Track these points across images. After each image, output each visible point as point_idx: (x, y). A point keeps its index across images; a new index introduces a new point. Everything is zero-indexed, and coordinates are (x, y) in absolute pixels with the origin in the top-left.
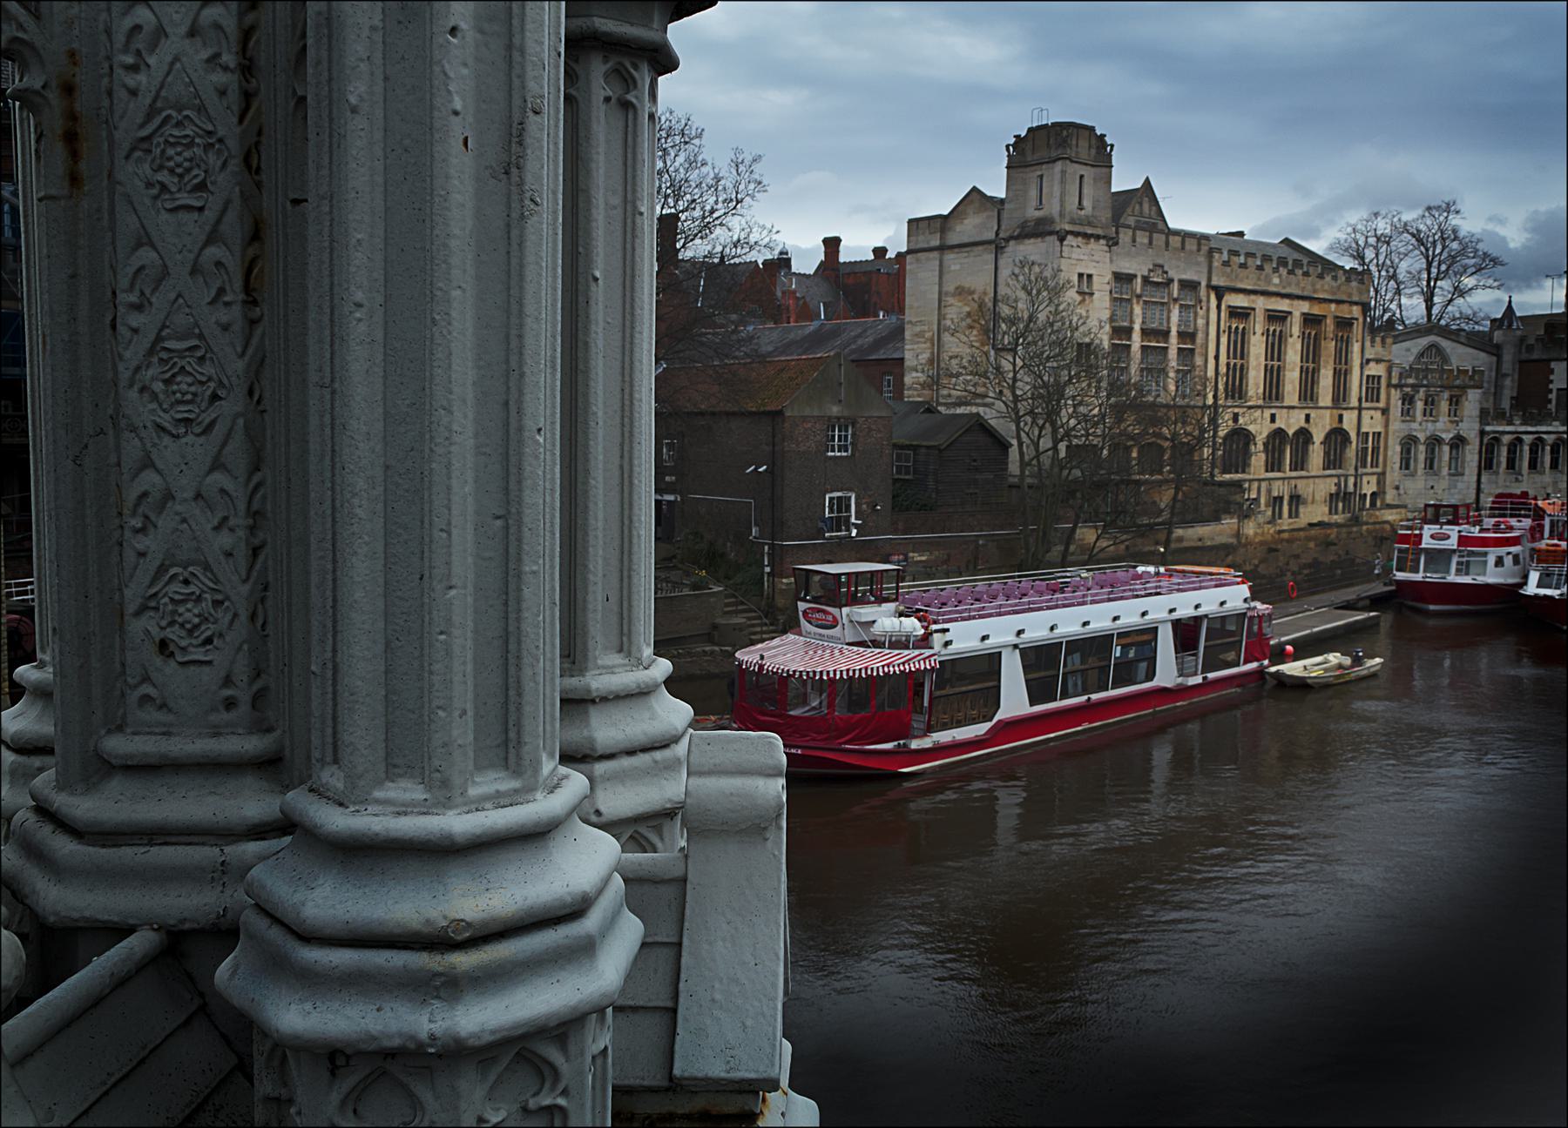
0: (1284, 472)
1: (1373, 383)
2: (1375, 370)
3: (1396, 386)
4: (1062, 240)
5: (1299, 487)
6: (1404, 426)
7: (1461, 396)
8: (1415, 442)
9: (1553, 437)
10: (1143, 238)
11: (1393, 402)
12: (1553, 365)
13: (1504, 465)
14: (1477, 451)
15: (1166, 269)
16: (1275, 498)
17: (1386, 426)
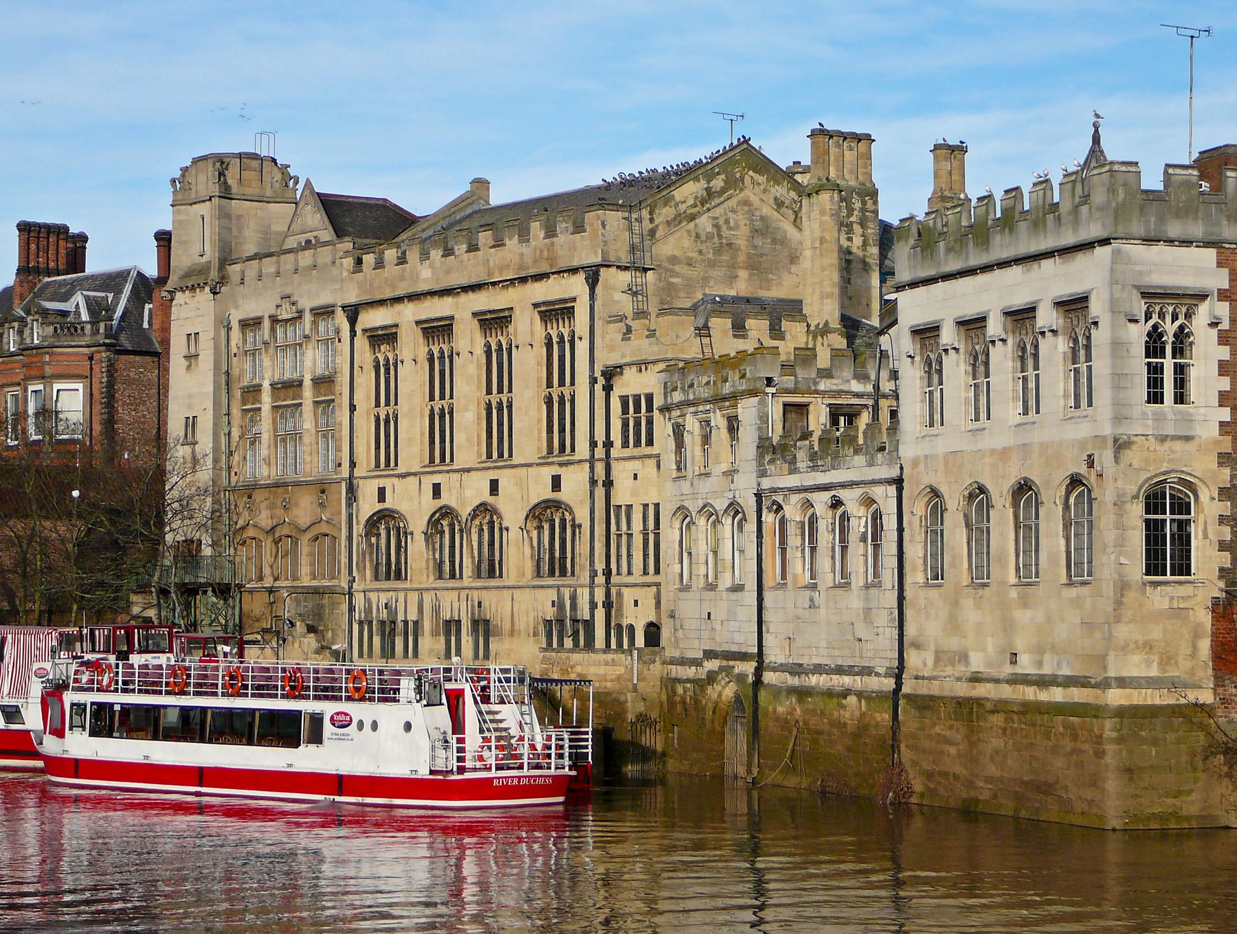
5: (485, 604)
15: (294, 299)
16: (448, 623)
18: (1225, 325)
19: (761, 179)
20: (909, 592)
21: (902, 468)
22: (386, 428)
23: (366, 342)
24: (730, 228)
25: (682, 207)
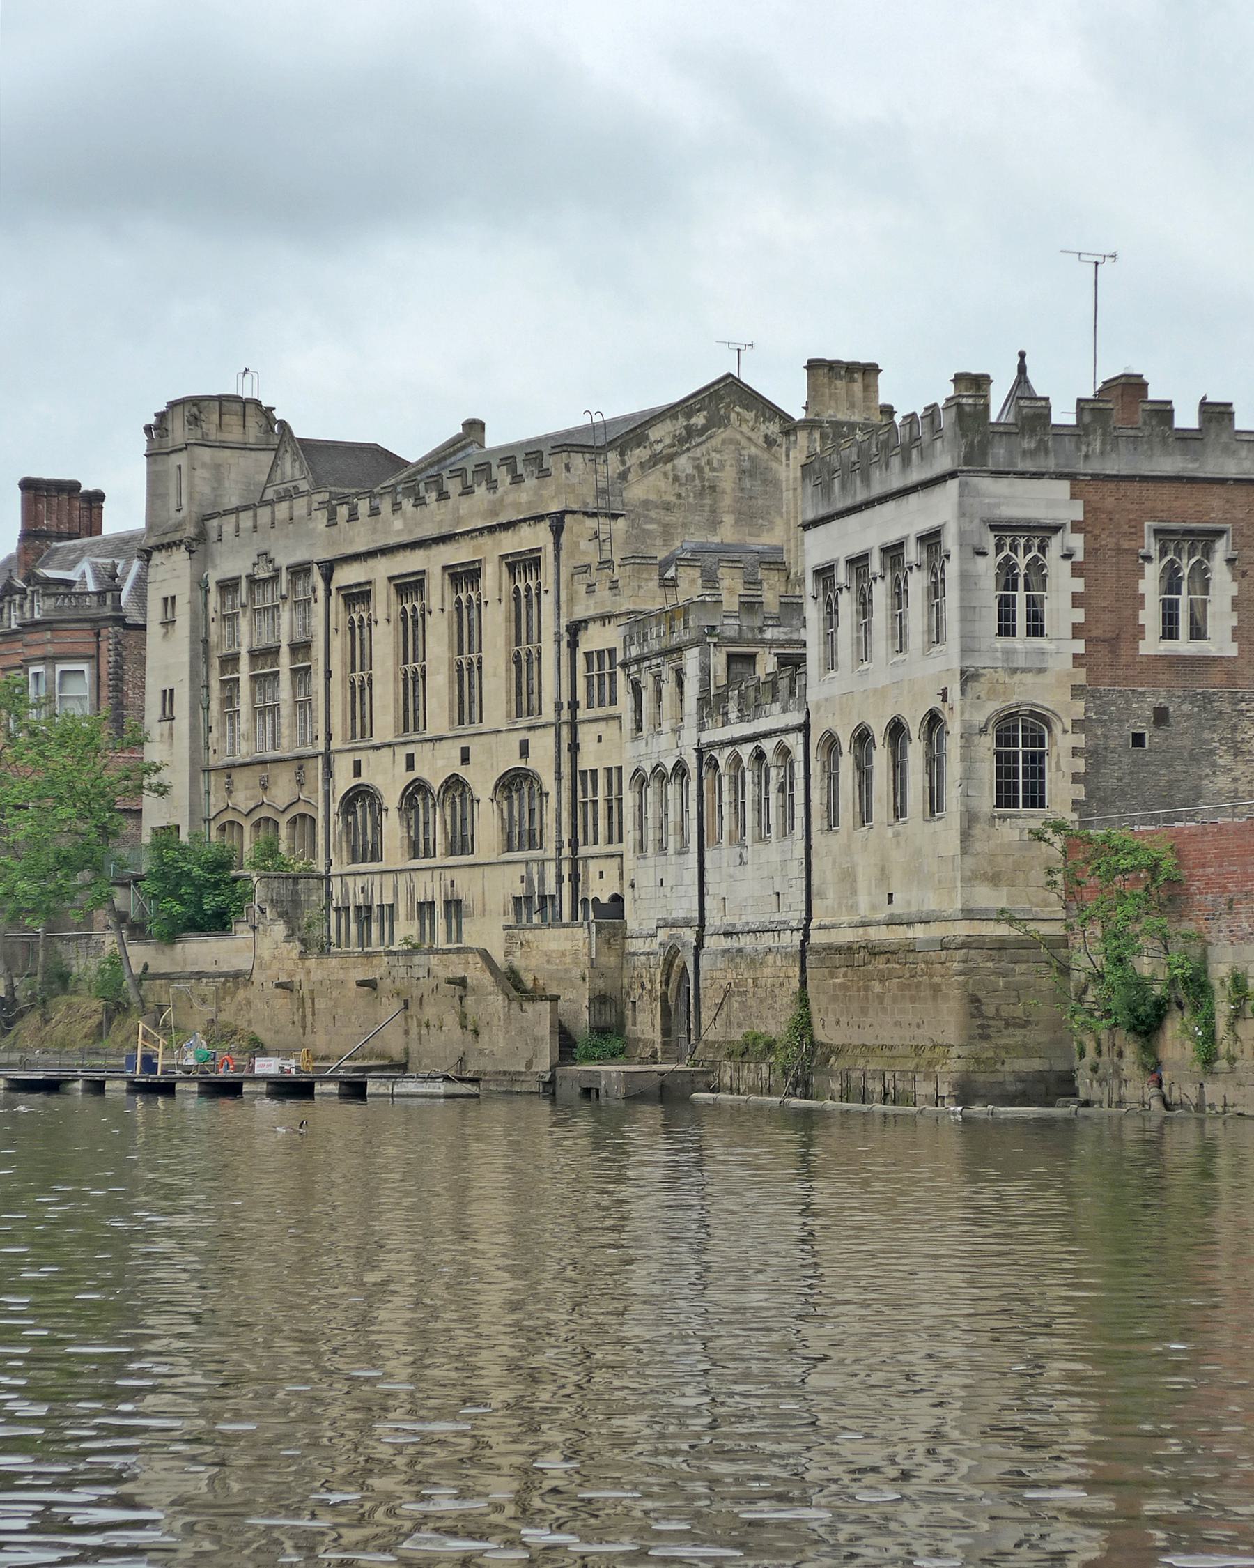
15: (272, 556)
16: (421, 904)
18: (1079, 557)
19: (750, 415)
21: (808, 713)
22: (360, 691)
23: (341, 600)
24: (713, 470)
25: (658, 447)
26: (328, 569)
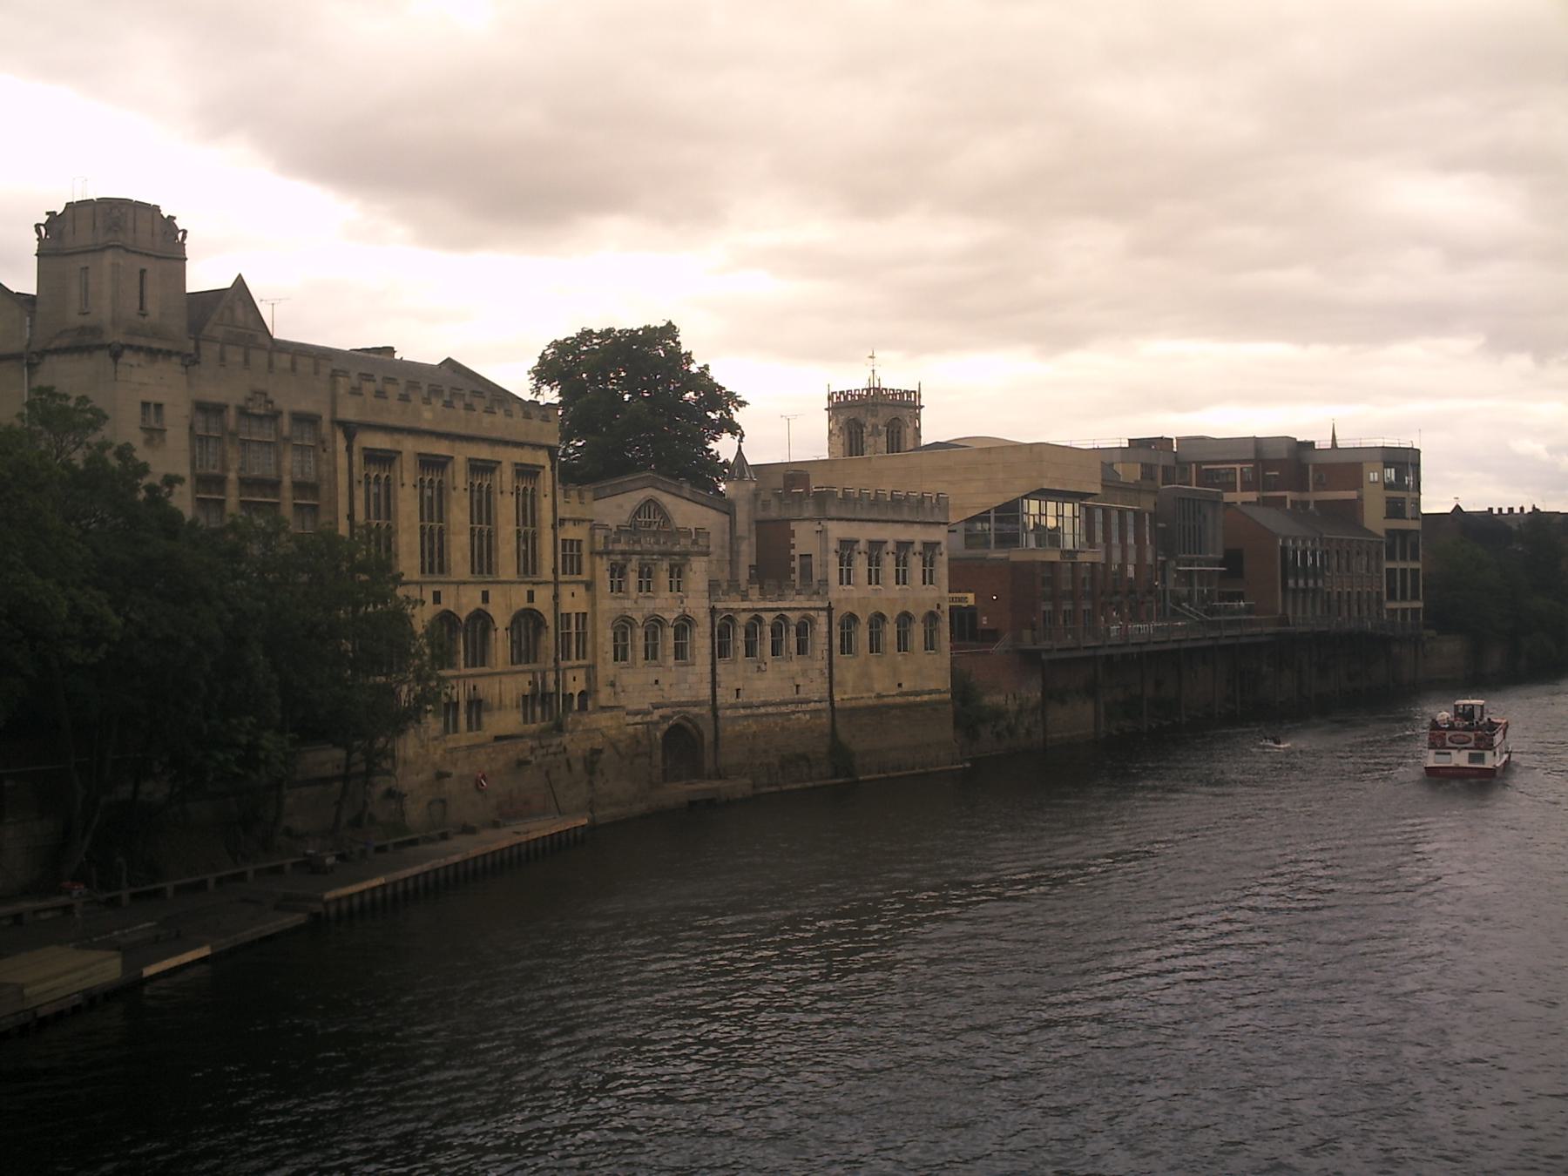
0: (459, 670)
1: (572, 550)
2: (571, 532)
3: (600, 554)
4: (116, 356)
5: (479, 687)
6: (615, 605)
7: (684, 565)
8: (630, 624)
9: (798, 614)
10: (233, 354)
11: (599, 573)
12: (793, 525)
13: (742, 650)
14: (708, 634)
15: (271, 396)
17: (593, 604)
20: (835, 660)
26: (350, 430)
